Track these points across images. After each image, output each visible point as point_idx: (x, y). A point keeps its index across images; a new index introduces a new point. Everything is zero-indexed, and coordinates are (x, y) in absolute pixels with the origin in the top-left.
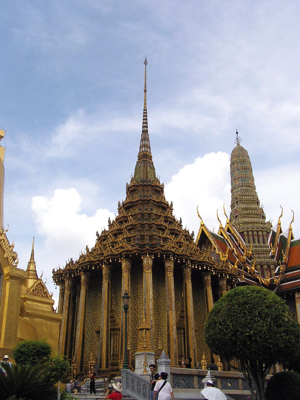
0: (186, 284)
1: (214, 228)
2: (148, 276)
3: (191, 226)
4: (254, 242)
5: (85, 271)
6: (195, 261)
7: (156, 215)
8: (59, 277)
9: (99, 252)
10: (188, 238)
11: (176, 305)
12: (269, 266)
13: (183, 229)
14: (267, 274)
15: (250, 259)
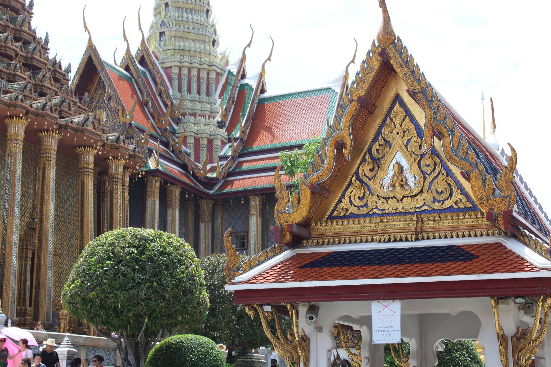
0: (44, 169)
1: (112, 55)
3: (67, 54)
4: (189, 91)
6: (66, 127)
11: (22, 206)
12: (210, 141)
14: (204, 155)
15: (177, 124)
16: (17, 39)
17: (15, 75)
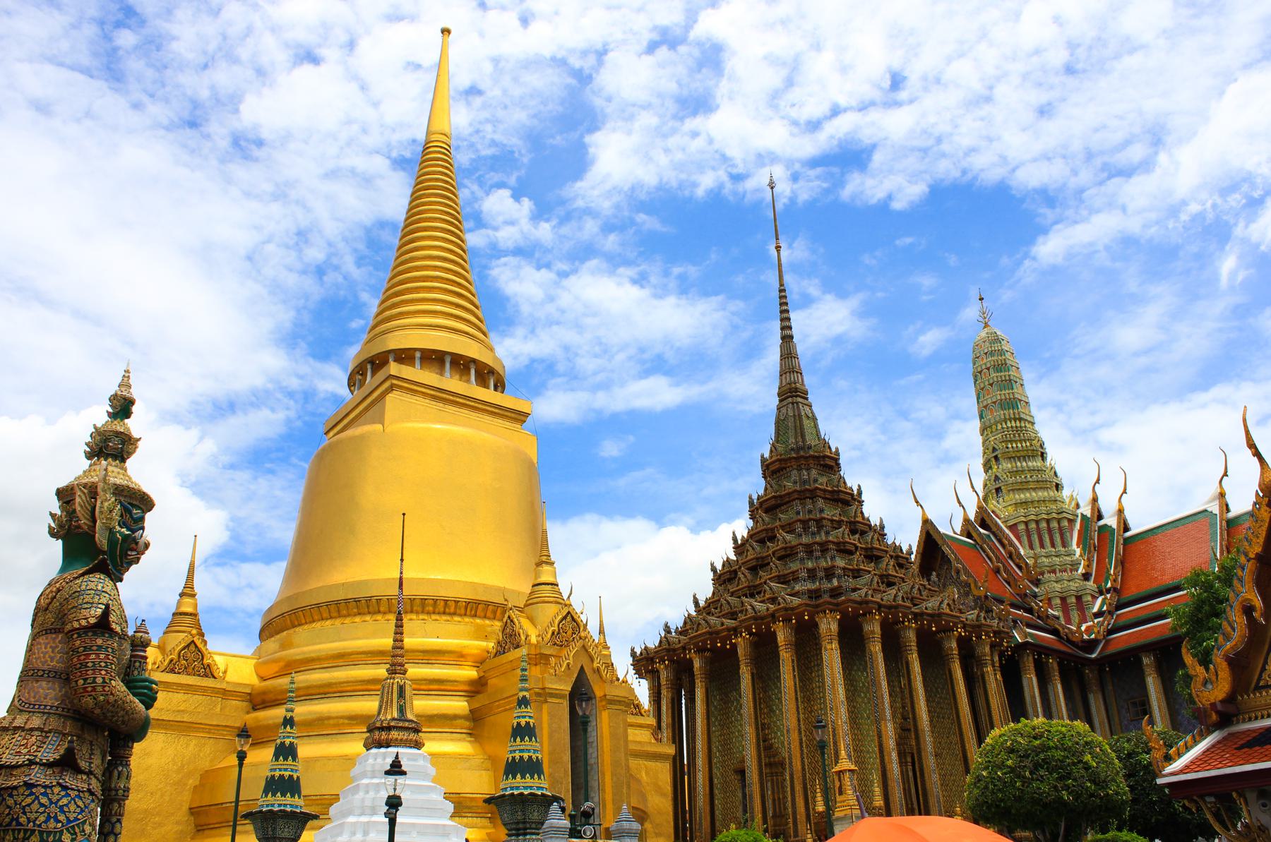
1: (950, 524)
2: (832, 656)
3: (906, 537)
4: (1042, 546)
5: (700, 650)
6: (922, 614)
7: (832, 521)
8: (644, 663)
9: (726, 609)
10: (901, 561)
12: (1079, 598)
13: (890, 542)
14: (1075, 615)
15: (1037, 585)
16: (853, 532)
17: (859, 570)
